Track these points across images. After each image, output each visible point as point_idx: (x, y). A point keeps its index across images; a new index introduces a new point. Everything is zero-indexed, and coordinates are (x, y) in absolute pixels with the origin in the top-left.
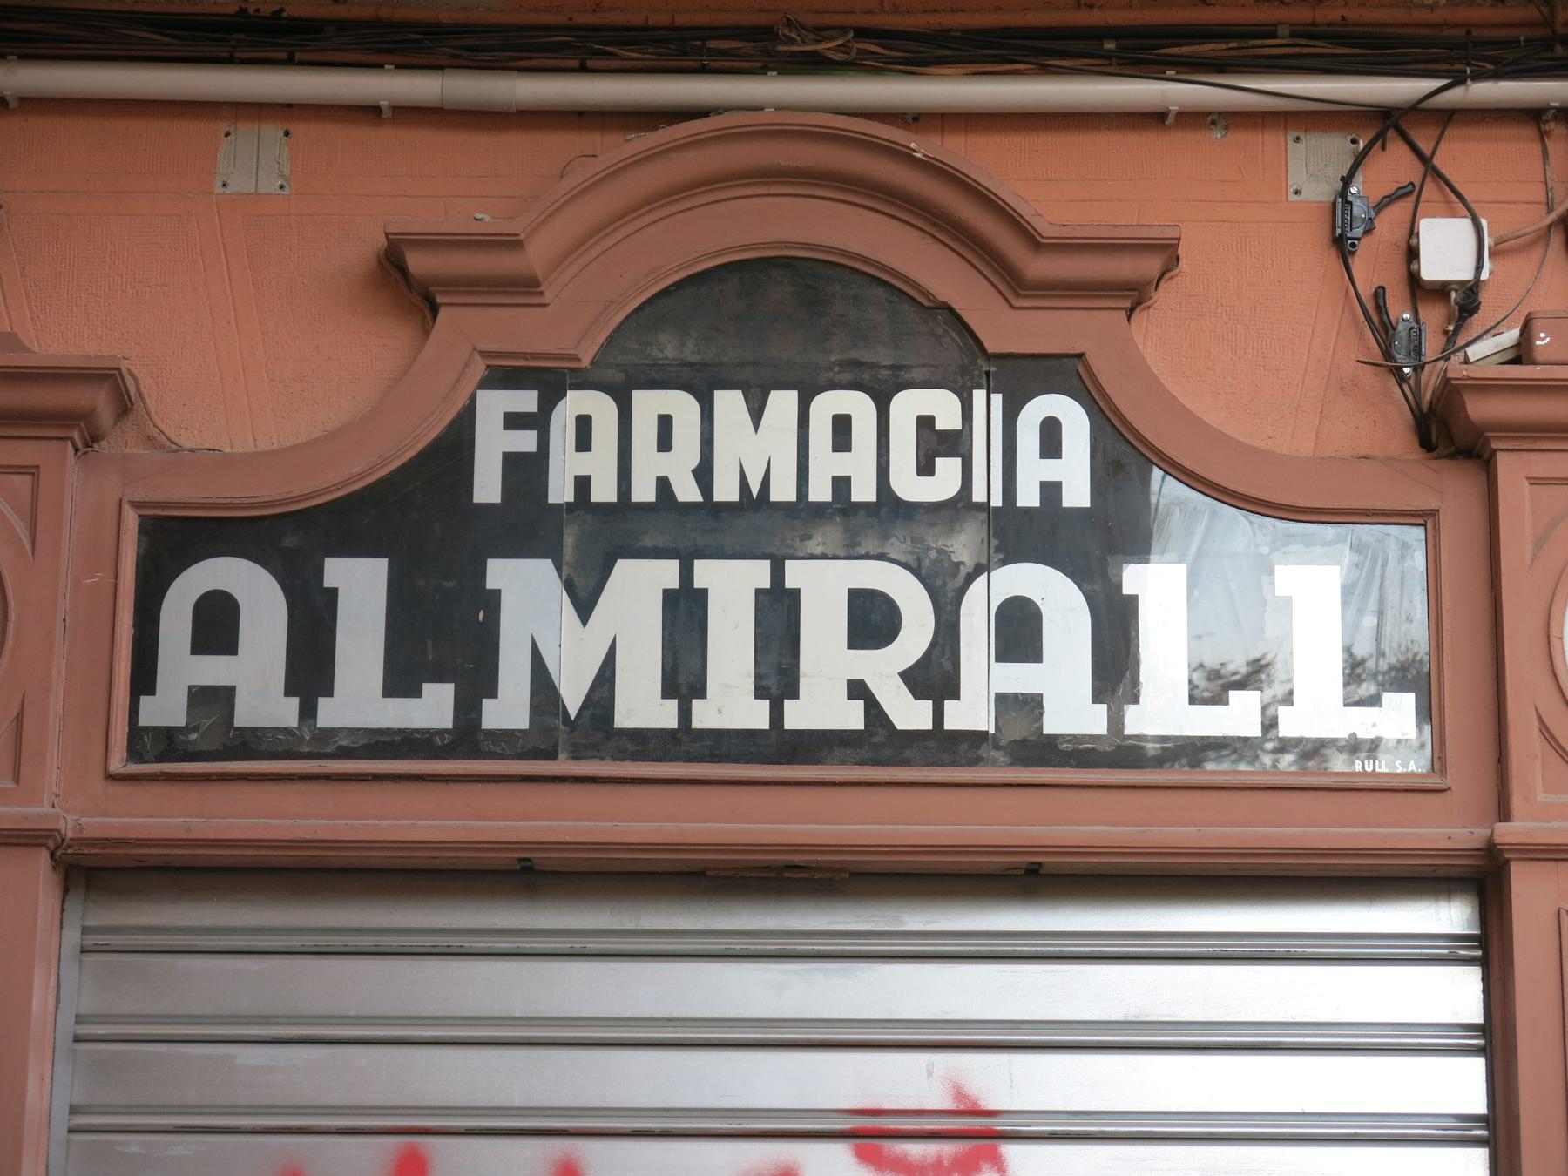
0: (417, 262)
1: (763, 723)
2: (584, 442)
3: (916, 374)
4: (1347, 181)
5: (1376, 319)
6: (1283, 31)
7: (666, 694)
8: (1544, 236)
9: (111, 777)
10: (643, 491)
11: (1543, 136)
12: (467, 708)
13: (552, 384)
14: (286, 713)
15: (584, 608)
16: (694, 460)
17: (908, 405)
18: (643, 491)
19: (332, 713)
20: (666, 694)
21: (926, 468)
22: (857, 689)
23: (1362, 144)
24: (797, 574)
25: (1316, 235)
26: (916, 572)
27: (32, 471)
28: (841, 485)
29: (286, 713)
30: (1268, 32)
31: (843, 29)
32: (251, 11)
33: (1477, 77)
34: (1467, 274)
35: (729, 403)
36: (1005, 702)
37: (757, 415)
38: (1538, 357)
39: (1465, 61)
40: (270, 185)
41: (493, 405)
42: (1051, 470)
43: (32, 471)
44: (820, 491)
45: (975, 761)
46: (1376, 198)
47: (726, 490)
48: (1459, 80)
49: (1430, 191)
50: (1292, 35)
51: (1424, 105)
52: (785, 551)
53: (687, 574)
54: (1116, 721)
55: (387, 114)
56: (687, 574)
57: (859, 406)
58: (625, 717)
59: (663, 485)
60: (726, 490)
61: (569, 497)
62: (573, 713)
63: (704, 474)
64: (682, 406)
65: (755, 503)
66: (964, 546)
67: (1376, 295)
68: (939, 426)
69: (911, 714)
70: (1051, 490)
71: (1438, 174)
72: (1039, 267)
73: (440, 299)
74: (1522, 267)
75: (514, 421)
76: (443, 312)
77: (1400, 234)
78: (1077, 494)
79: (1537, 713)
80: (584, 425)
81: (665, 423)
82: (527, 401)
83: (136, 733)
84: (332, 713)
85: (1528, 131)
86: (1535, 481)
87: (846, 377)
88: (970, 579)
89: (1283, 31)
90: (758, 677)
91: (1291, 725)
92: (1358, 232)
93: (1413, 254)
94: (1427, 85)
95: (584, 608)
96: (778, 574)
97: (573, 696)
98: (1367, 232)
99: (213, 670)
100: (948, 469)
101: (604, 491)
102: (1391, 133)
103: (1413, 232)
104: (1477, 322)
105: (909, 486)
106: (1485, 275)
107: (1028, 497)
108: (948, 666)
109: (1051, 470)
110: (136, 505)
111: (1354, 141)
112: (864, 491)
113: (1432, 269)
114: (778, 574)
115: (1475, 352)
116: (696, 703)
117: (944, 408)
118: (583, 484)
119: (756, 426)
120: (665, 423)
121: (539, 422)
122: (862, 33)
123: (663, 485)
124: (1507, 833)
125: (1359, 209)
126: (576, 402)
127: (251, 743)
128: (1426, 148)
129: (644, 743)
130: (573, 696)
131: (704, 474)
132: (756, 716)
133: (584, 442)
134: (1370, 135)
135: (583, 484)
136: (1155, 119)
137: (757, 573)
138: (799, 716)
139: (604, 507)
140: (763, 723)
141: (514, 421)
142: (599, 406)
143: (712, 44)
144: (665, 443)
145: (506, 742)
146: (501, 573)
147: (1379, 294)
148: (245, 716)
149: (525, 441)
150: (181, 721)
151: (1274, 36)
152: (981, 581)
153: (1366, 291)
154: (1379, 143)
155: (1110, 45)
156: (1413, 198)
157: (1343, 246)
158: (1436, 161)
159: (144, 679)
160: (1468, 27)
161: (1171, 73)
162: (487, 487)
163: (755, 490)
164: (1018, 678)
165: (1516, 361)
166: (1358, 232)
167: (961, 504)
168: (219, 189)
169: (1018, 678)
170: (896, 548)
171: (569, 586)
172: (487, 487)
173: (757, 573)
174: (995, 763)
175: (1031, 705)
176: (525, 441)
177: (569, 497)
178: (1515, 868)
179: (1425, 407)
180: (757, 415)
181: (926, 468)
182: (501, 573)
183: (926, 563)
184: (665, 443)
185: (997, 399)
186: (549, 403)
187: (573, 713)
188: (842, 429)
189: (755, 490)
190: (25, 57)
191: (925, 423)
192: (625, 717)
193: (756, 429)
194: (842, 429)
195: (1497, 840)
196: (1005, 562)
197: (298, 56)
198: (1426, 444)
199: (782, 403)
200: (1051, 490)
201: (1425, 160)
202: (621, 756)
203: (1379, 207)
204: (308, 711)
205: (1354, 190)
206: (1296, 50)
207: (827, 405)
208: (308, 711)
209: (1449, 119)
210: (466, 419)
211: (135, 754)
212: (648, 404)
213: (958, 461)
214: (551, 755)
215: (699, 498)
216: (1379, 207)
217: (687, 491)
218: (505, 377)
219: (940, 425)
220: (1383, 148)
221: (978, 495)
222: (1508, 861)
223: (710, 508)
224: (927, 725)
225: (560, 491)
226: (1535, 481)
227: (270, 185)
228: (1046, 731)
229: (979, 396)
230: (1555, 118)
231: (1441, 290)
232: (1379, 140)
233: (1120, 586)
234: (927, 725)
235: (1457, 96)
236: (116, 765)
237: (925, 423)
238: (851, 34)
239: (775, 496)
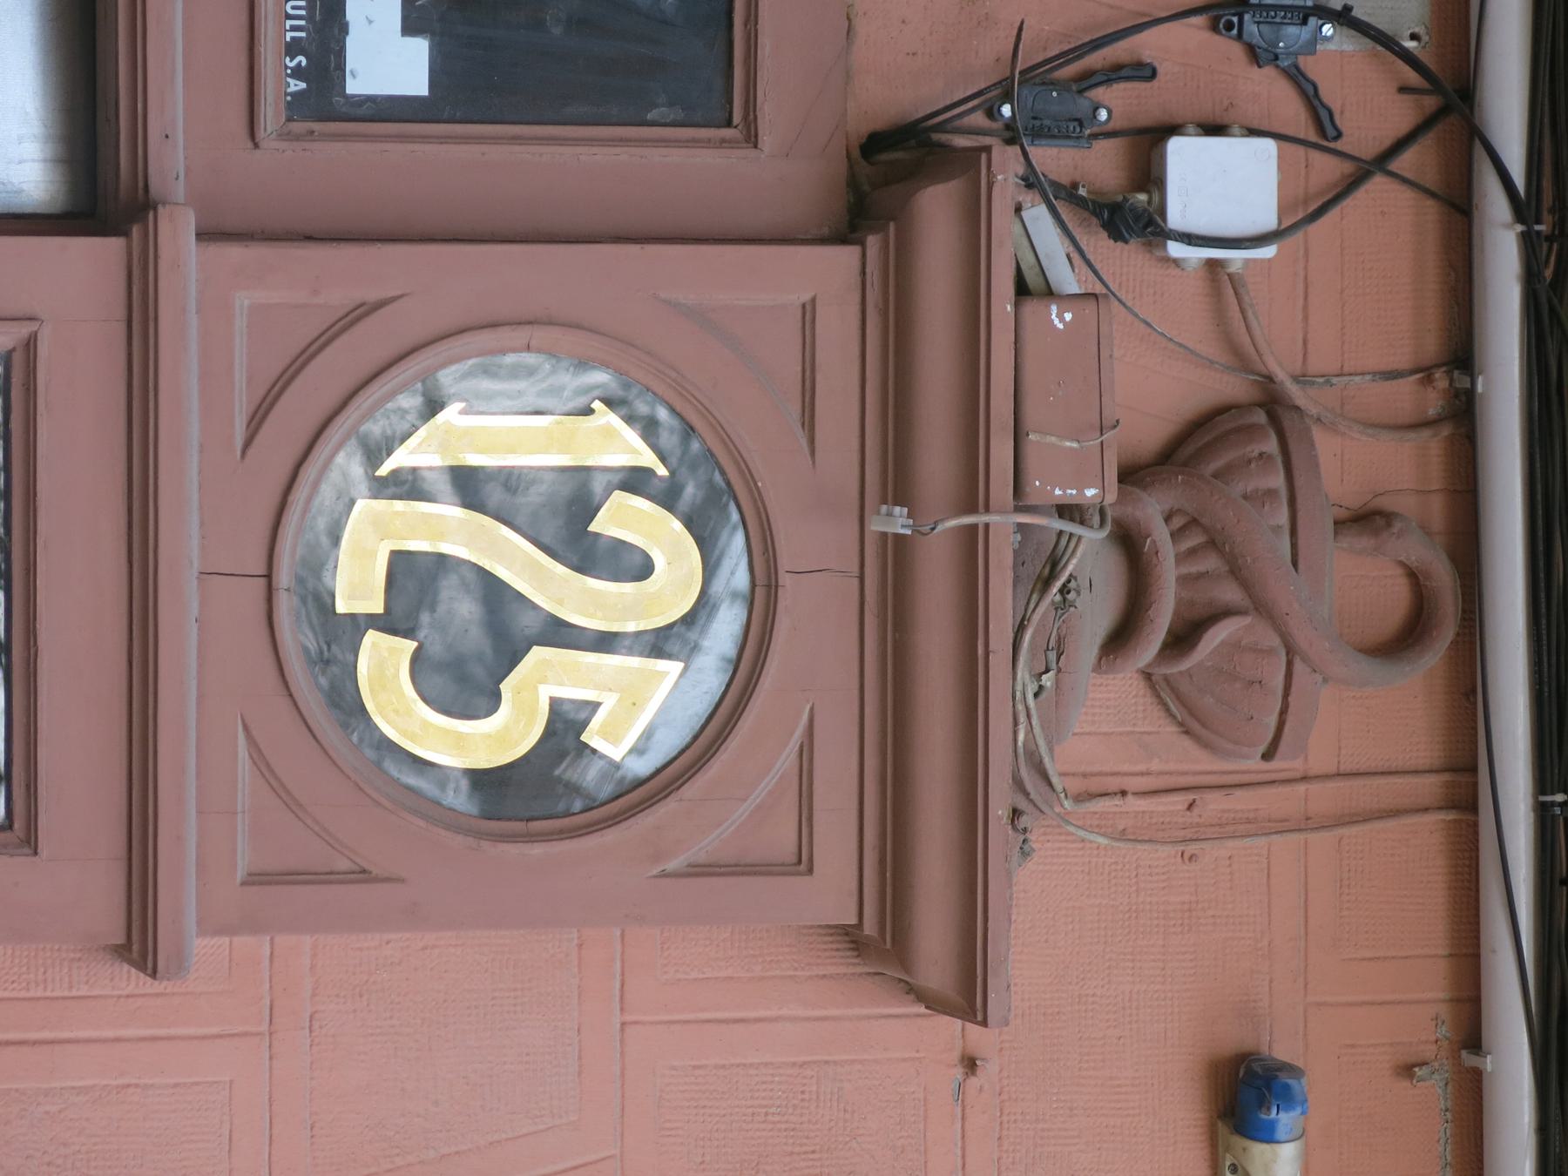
4: (1344, 18)
5: (1095, 60)
8: (1241, 361)
11: (1425, 372)
23: (1411, 45)
33: (1528, 242)
34: (1178, 215)
38: (1031, 307)
39: (1557, 232)
46: (1308, 65)
48: (1522, 210)
49: (1327, 169)
51: (1480, 153)
67: (1139, 65)
74: (1196, 330)
79: (401, 296)
85: (1431, 346)
86: (808, 312)
93: (1215, 129)
94: (1514, 152)
98: (1255, 55)
102: (1431, 103)
104: (1098, 244)
106: (1175, 249)
111: (1414, 37)
115: (1039, 217)
128: (1405, 162)
134: (1426, 58)
147: (1143, 72)
153: (1147, 45)
154: (1412, 77)
156: (1313, 137)
158: (1378, 182)
165: (1022, 289)
178: (114, 245)
179: (936, 137)
198: (875, 144)
201: (1382, 161)
203: (1297, 77)
205: (1327, 29)
209: (1453, 205)
216: (1297, 77)
220: (1403, 89)
222: (126, 234)
226: (808, 312)
231: (1149, 175)
235: (1495, 207)
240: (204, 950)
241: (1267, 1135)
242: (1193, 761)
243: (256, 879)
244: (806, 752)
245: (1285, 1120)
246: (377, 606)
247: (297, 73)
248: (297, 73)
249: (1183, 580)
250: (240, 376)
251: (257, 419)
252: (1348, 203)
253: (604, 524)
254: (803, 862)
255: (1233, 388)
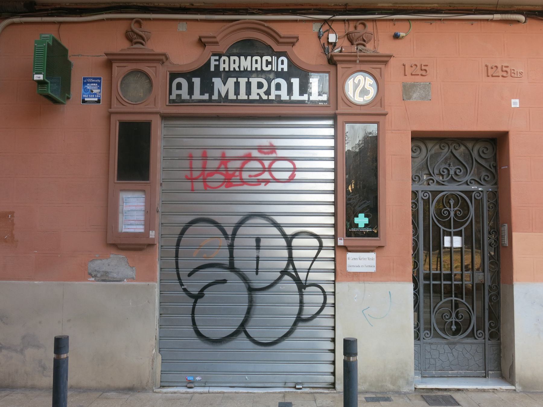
0: (203, 40)
1: (247, 98)
2: (224, 63)
3: (266, 54)
4: (320, 29)
5: (323, 47)
6: (313, 9)
7: (235, 95)
8: (344, 37)
9: (167, 106)
10: (232, 69)
11: (345, 23)
12: (210, 96)
13: (220, 56)
14: (188, 97)
15: (225, 84)
16: (238, 65)
17: (265, 58)
18: (232, 69)
19: (194, 97)
20: (235, 95)
21: (267, 66)
22: (258, 94)
24: (251, 80)
25: (316, 37)
26: (266, 79)
27: (156, 67)
28: (256, 68)
29: (188, 97)
30: (310, 9)
31: (256, 9)
32: (181, 7)
33: (337, 15)
34: (334, 41)
35: (242, 58)
36: (276, 96)
37: (246, 60)
38: (343, 52)
40: (184, 30)
41: (213, 58)
42: (282, 66)
43: (156, 67)
44: (254, 69)
45: (273, 103)
46: (323, 32)
47: (242, 69)
48: (334, 16)
49: (330, 30)
50: (314, 10)
51: (330, 19)
52: (249, 77)
53: (237, 80)
54: (290, 98)
55: (199, 20)
56: (237, 80)
57: (258, 58)
58: (229, 98)
59: (234, 68)
60: (242, 69)
61: (222, 70)
62: (223, 97)
63: (239, 67)
64: (236, 58)
65: (246, 71)
66: (272, 76)
67: (323, 44)
68: (269, 61)
69: (265, 97)
70: (282, 69)
71: (331, 28)
72: (281, 40)
73: (206, 45)
74: (342, 40)
75: (215, 60)
76: (206, 46)
77: (327, 36)
78: (286, 69)
80: (224, 61)
81: (234, 61)
82: (217, 58)
83: (170, 100)
84: (194, 97)
85: (343, 23)
86: (342, 68)
87: (257, 55)
88: (272, 80)
89: (313, 9)
90: (246, 93)
91: (312, 98)
92: (321, 36)
93: (328, 39)
94: (330, 16)
95: (225, 84)
96: (248, 80)
97: (223, 95)
98: (323, 36)
99: (179, 92)
100: (270, 66)
101: (227, 69)
102: (326, 23)
103: (328, 36)
104: (336, 47)
105: (265, 68)
106: (337, 41)
107: (280, 70)
108: (269, 91)
109: (282, 66)
110: (169, 71)
112: (259, 69)
113: (330, 41)
114: (248, 80)
115: (335, 51)
116: (238, 96)
117: (269, 58)
118: (224, 68)
119: (246, 61)
120: (234, 61)
121: (219, 60)
122: (259, 9)
123: (234, 68)
124: (337, 112)
125: (321, 33)
126: (223, 58)
127: (184, 101)
128: (330, 25)
129: (232, 101)
130: (223, 95)
131: (239, 67)
132: (246, 97)
133: (224, 63)
134: (323, 23)
135: (224, 68)
136: (296, 21)
137: (246, 80)
138: (251, 97)
139: (227, 71)
140: (247, 98)
141: (215, 60)
142: (226, 58)
143: (240, 11)
144: (234, 63)
145: (215, 101)
146: (214, 80)
147: (324, 44)
148: (183, 98)
149: (217, 63)
150: (175, 98)
151: (311, 10)
152: (274, 80)
153: (322, 43)
155: (290, 11)
157: (319, 38)
158: (331, 26)
159: (170, 93)
160: (336, 9)
161: (298, 15)
162: (212, 69)
163: (246, 69)
164: (278, 93)
165: (340, 52)
166: (321, 36)
167: (271, 71)
168: (178, 30)
169: (278, 93)
170: (263, 76)
171: (223, 81)
172: (212, 69)
173: (246, 80)
174: (275, 103)
175: (279, 96)
176: (217, 63)
177: (222, 70)
178: (338, 116)
179: (329, 58)
180: (246, 60)
181: (267, 66)
182: (214, 80)
183: (267, 78)
184: (234, 63)
185: (276, 57)
186: (220, 57)
187: (223, 97)
188: (256, 61)
189: (246, 69)
190: (153, 13)
191: (267, 60)
192: (229, 98)
193: (246, 61)
194: (256, 61)
195: (336, 113)
196: (277, 78)
197: (188, 13)
198: (329, 63)
199: (249, 58)
200: (282, 69)
201: (330, 26)
202: (229, 103)
203: (324, 32)
204: (191, 97)
205: (321, 30)
206: (314, 12)
207: (255, 58)
208: (191, 97)
210: (210, 59)
211: (170, 103)
212: (232, 58)
213: (271, 65)
214: (221, 102)
215: (239, 70)
216: (324, 32)
217: (237, 69)
218: (214, 55)
219: (269, 61)
221: (273, 70)
222: (337, 115)
223: (240, 71)
224: (267, 99)
225: (221, 69)
226: (342, 68)
227: (184, 30)
228: (281, 99)
229: (274, 57)
230: (346, 21)
231: (331, 43)
232: (324, 23)
233: (291, 81)
234: (267, 99)
235: (334, 18)
236: (167, 104)
237: (267, 60)
238: (257, 10)
239: (248, 70)
240: (386, 110)
241: (400, 35)
242: (372, 41)
243: (381, 107)
244: (373, 68)
245: (399, 34)
246: (362, 98)
247: (325, 103)
248: (325, 103)
249: (360, 41)
250: (347, 108)
251: (350, 107)
252: (333, 29)
253: (357, 83)
254: (380, 68)
255: (346, 37)
